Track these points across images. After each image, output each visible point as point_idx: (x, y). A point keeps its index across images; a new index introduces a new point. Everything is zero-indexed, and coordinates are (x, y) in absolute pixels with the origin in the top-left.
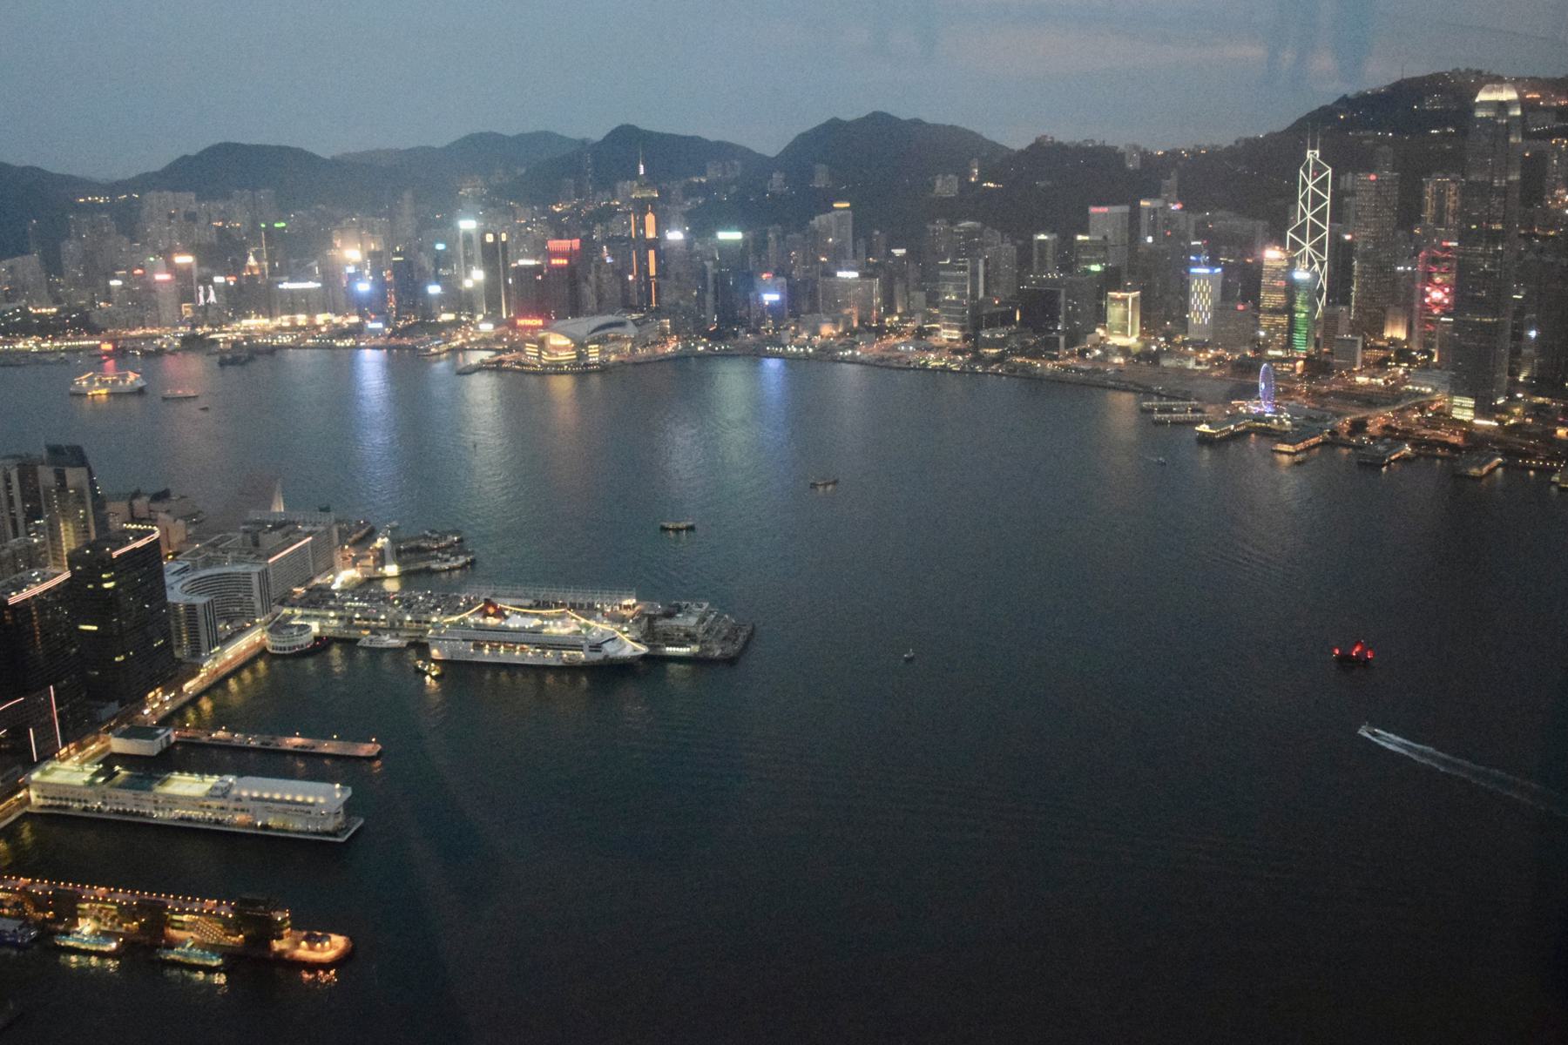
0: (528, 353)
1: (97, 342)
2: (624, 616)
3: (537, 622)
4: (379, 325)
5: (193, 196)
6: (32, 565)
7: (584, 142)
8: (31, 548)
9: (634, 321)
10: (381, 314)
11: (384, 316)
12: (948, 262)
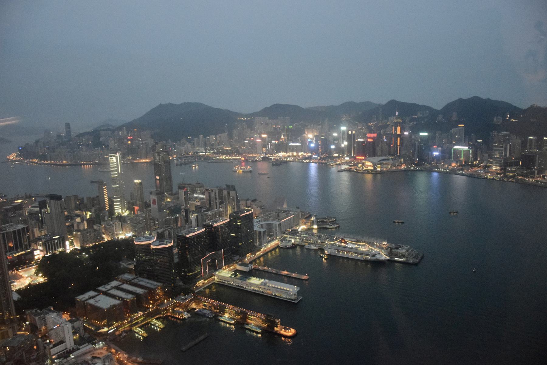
1: (240, 158)
2: (383, 247)
3: (356, 246)
4: (316, 156)
5: (268, 118)
6: (220, 216)
7: (380, 105)
8: (220, 212)
9: (392, 159)
10: (317, 153)
11: (317, 154)
12: (497, 145)
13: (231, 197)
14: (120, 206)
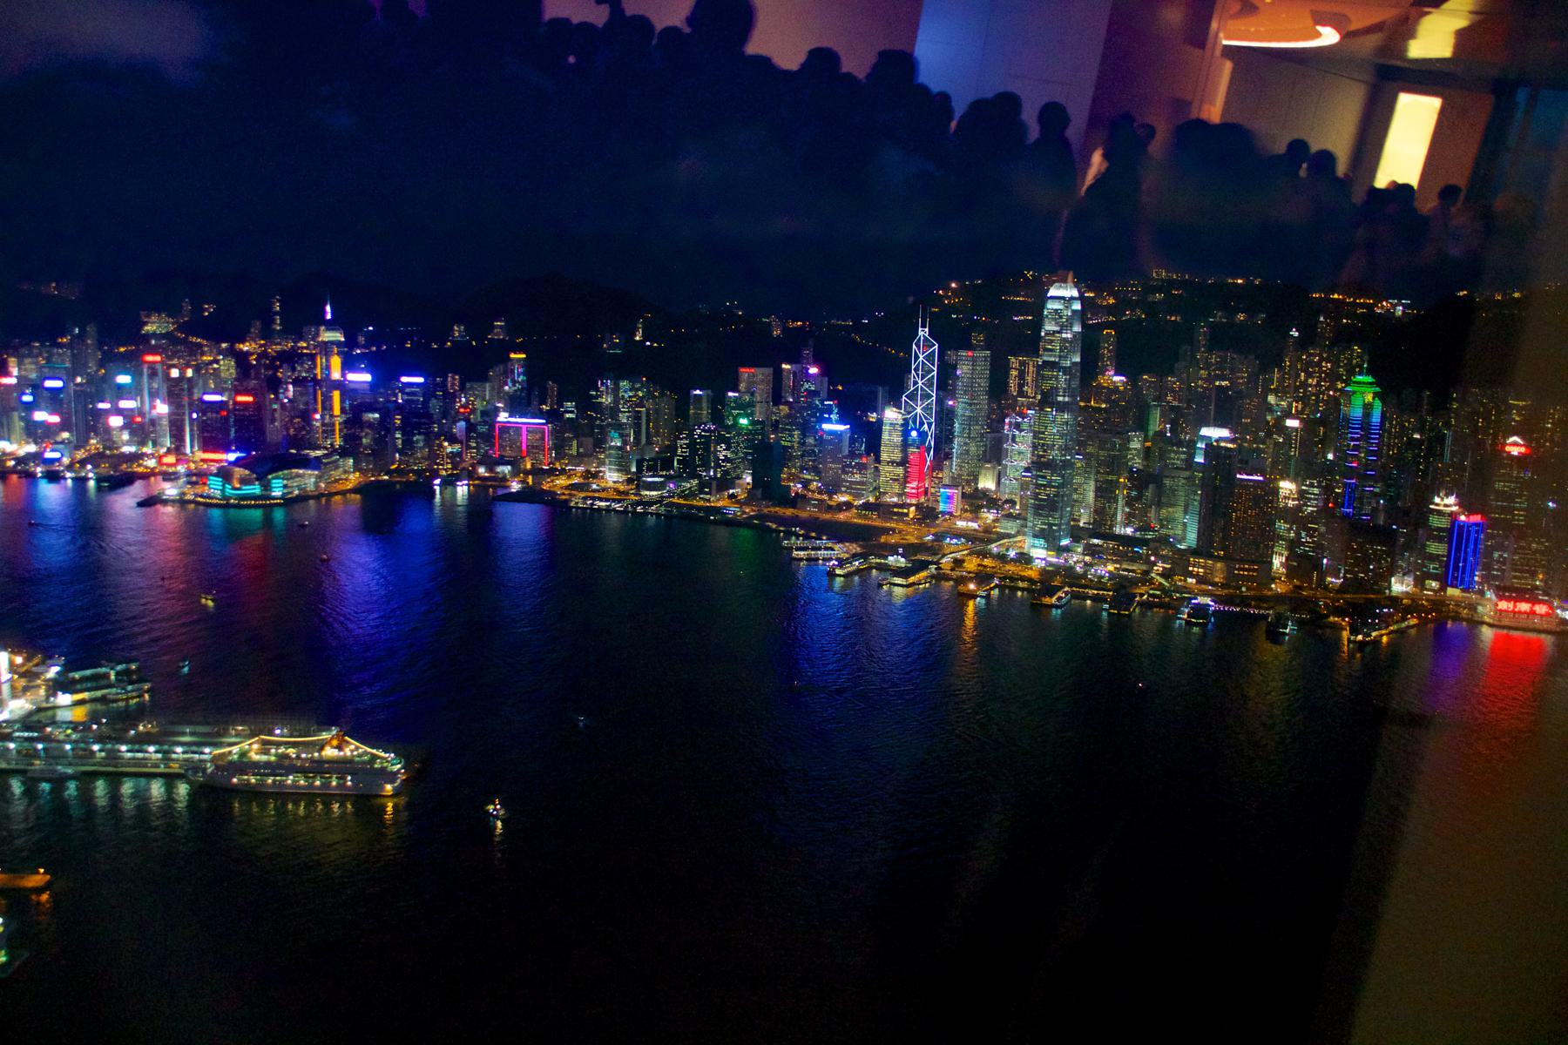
0: (212, 486)
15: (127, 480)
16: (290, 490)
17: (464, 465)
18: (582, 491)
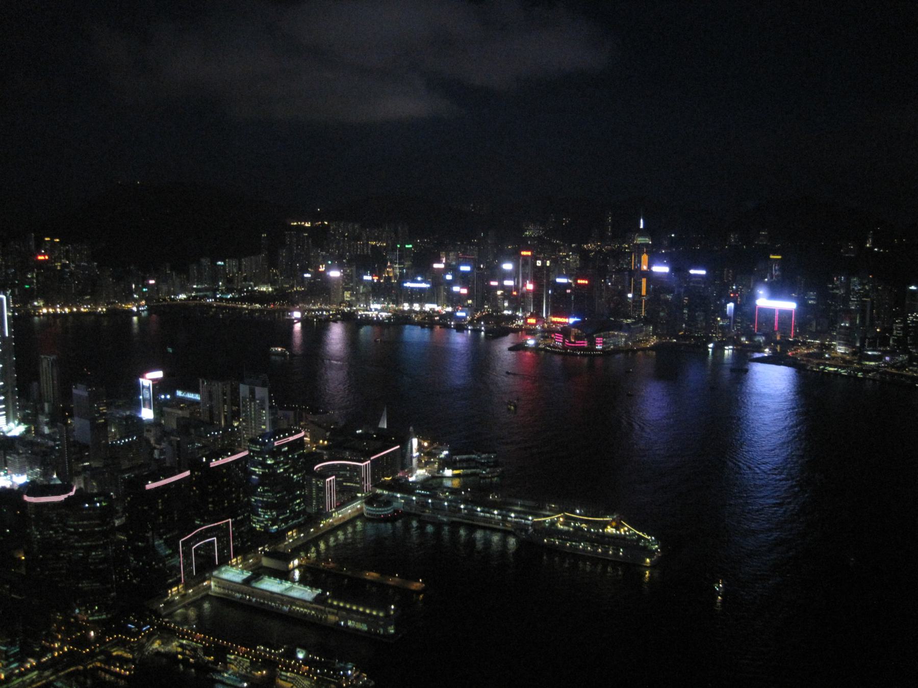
13: (258, 401)
14: (4, 413)
15: (506, 332)
16: (608, 346)
17: (732, 334)
18: (817, 358)
